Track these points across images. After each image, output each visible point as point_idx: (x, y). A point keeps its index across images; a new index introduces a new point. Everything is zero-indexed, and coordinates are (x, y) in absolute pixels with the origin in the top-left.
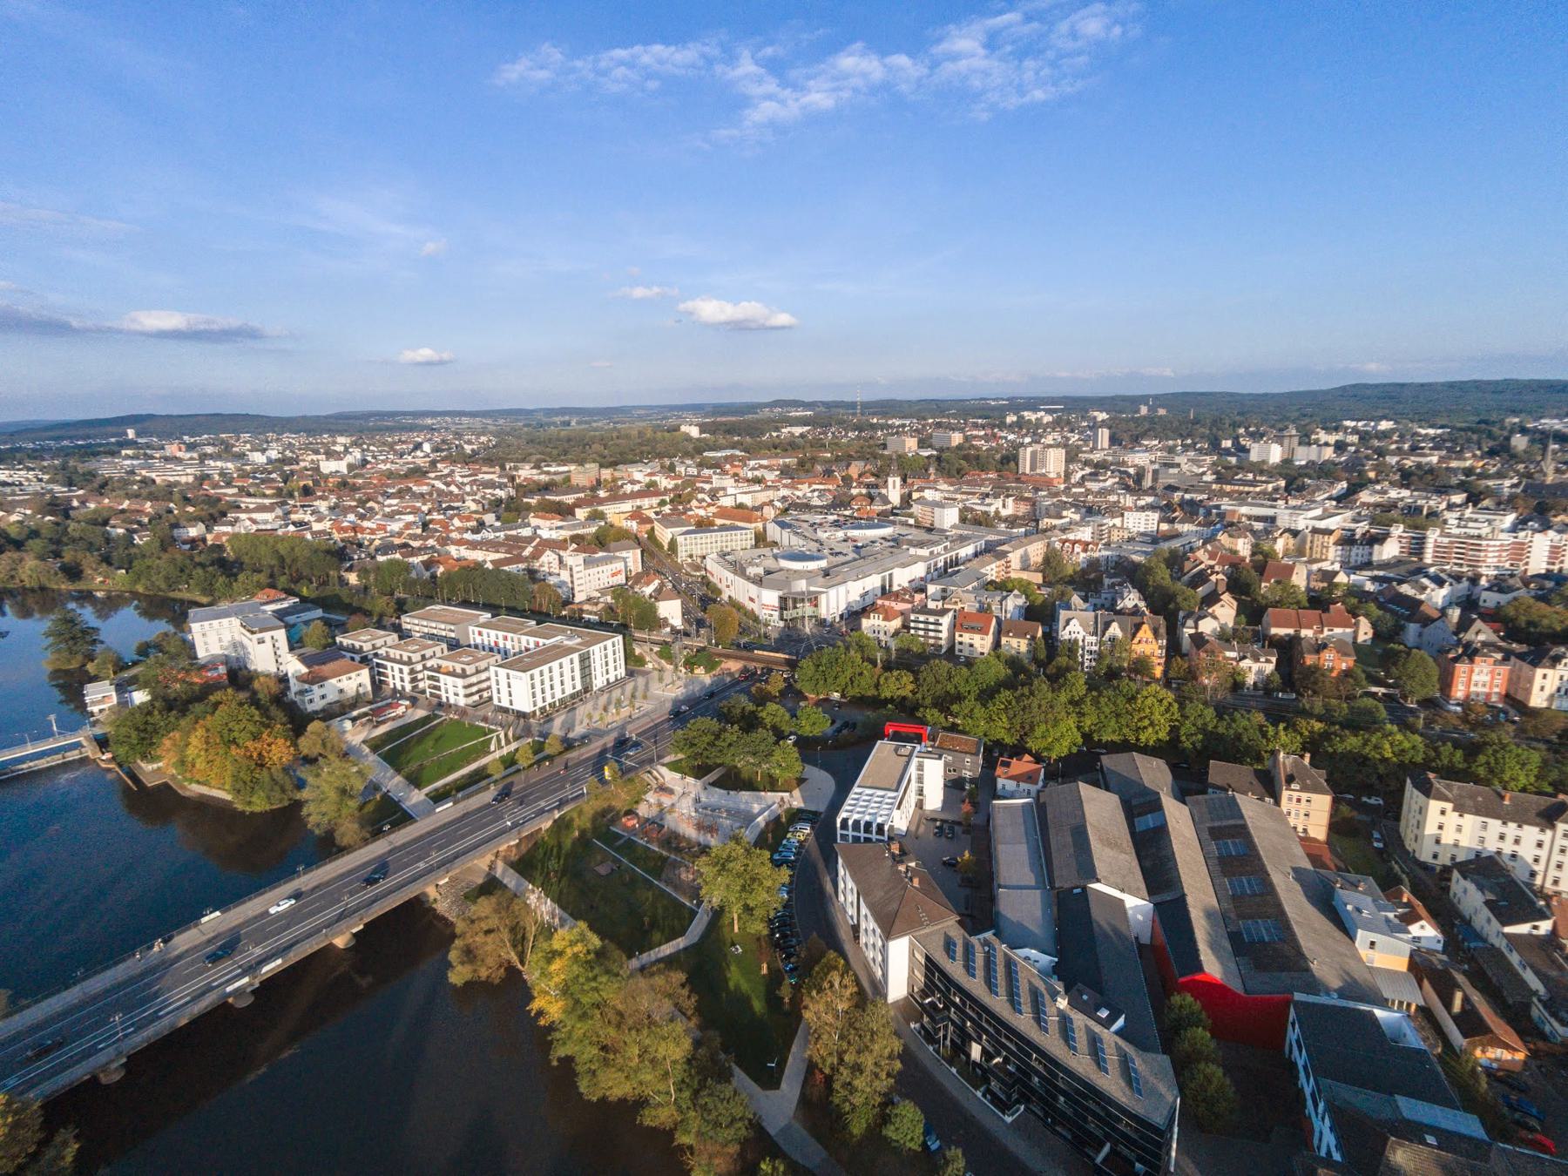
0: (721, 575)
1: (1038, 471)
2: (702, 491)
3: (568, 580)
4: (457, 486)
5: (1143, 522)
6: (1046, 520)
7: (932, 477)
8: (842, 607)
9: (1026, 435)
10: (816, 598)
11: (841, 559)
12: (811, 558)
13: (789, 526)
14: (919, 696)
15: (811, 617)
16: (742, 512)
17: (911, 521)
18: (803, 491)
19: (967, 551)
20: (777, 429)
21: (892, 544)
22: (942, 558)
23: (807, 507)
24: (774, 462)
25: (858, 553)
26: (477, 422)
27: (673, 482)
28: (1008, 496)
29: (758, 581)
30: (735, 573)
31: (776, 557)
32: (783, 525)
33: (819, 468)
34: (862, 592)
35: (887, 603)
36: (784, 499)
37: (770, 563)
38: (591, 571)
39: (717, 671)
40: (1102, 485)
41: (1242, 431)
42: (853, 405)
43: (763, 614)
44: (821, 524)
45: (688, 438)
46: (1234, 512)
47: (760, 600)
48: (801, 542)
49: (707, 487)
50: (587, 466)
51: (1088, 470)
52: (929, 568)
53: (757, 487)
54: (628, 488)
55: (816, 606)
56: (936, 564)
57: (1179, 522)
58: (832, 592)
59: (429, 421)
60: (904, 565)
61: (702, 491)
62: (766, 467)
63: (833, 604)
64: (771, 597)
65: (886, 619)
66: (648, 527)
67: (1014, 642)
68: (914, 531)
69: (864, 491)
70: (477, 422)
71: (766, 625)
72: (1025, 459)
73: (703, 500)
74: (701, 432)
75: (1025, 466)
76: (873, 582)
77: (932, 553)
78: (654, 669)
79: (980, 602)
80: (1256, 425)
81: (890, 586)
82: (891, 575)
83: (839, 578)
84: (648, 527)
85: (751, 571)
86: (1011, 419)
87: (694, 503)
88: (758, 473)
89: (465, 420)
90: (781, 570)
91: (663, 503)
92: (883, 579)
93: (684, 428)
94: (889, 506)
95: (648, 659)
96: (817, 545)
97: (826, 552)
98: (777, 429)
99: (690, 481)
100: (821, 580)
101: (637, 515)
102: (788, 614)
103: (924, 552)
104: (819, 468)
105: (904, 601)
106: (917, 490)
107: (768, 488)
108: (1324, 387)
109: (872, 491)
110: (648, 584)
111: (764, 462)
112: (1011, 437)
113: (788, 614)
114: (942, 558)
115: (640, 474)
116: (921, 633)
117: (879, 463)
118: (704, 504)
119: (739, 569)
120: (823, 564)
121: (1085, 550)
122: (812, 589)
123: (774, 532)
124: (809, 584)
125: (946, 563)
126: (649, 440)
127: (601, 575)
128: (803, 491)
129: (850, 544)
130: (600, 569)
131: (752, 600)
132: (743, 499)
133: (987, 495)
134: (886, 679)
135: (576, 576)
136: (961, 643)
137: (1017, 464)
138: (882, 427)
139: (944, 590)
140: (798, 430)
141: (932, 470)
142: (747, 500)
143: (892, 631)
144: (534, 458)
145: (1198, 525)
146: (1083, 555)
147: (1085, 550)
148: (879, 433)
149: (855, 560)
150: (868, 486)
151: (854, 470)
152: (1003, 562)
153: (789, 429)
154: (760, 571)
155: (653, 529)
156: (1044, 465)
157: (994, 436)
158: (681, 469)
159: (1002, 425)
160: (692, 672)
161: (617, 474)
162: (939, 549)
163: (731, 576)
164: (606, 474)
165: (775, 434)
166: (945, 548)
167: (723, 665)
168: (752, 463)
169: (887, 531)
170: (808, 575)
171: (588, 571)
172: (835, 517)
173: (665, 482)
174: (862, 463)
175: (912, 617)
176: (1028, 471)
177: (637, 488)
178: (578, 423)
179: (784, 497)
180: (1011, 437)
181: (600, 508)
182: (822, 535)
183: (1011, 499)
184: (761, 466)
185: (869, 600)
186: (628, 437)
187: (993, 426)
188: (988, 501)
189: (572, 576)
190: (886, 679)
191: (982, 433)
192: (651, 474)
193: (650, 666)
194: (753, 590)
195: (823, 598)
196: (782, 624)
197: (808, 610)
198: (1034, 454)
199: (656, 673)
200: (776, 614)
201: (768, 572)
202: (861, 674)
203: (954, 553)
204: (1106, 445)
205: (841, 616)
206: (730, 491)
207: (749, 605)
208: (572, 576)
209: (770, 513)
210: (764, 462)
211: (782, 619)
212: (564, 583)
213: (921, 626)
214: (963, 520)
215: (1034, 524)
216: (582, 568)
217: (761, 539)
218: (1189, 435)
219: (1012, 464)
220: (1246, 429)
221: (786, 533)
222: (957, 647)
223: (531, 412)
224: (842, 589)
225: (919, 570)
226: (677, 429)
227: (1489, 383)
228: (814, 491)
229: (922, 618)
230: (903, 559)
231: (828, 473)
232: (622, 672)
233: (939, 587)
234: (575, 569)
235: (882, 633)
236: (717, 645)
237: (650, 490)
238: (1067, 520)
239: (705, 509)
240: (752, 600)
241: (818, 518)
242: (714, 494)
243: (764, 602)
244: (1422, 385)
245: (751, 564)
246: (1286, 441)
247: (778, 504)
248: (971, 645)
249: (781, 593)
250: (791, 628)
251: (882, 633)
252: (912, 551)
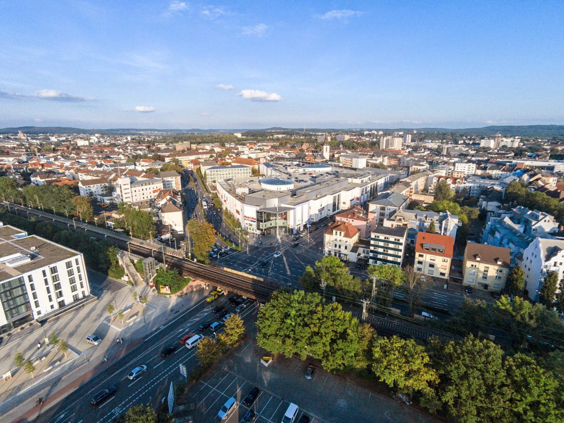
0: (223, 193)
1: (390, 148)
2: (233, 153)
3: (120, 194)
4: (123, 149)
5: (466, 169)
6: (414, 167)
7: (342, 149)
8: (306, 219)
9: (373, 138)
10: (286, 213)
11: (303, 184)
12: (283, 183)
13: (272, 166)
14: (449, 397)
15: (281, 227)
16: (249, 161)
17: (341, 165)
18: (281, 153)
19: (381, 182)
20: (272, 135)
21: (334, 176)
22: (369, 185)
23: (283, 159)
24: (269, 144)
25: (315, 181)
26: (160, 133)
27: (221, 150)
28: (384, 156)
29: (241, 199)
30: (229, 192)
31: (260, 182)
32: (267, 165)
33: (289, 146)
34: (320, 208)
35: (344, 219)
36: (271, 156)
37: (255, 186)
38: (137, 189)
39: (185, 290)
40: (422, 154)
41: (464, 138)
42: (302, 130)
43: (244, 224)
44: (289, 166)
45: (236, 137)
46: (523, 163)
47: (243, 213)
48: (278, 174)
49: (236, 151)
50: (185, 142)
51: (410, 150)
52: (362, 192)
53: (259, 151)
54: (201, 151)
55: (286, 219)
56: (366, 188)
57: (490, 169)
58: (298, 208)
59: (142, 132)
60: (348, 189)
61: (233, 153)
62: (267, 146)
63: (299, 217)
64: (251, 211)
65: (347, 235)
66: (198, 166)
67: (482, 267)
68: (343, 169)
69: (311, 154)
70: (160, 133)
71: (247, 233)
72: (383, 143)
73: (232, 156)
74: (242, 136)
75: (383, 146)
76: (328, 200)
77: (362, 181)
78: (129, 282)
79: (420, 220)
80: (470, 136)
81: (338, 204)
82: (339, 196)
83: (303, 198)
84: (198, 166)
85: (239, 191)
86: (366, 133)
87: (227, 157)
88: (261, 148)
89: (156, 132)
90: (262, 190)
91: (211, 156)
92: (335, 199)
93: (235, 134)
94: (324, 160)
95: (126, 271)
96: (288, 176)
97: (293, 179)
98: (272, 135)
99: (229, 151)
100: (289, 198)
101: (195, 162)
102: (263, 225)
103: (358, 181)
104: (289, 146)
105: (359, 218)
106: (337, 153)
107: (264, 151)
108: (481, 127)
109: (315, 154)
110: (162, 199)
111: (265, 144)
112: (367, 139)
113: (263, 225)
114: (369, 185)
115: (208, 147)
116: (381, 250)
117: (316, 144)
118: (232, 158)
119: (232, 191)
120: (291, 187)
121: (454, 182)
122: (283, 205)
123: (263, 169)
124: (280, 202)
125: (371, 188)
126: (220, 138)
127: (145, 191)
128: (281, 153)
129: (308, 176)
130: (144, 187)
131: (238, 212)
132: (250, 155)
133: (373, 156)
134: (385, 352)
135: (124, 192)
136: (420, 263)
137: (379, 145)
138: (314, 135)
139: (383, 209)
140: (280, 136)
141: (341, 146)
142: (253, 156)
143: (352, 245)
144: (168, 142)
145: (504, 170)
146: (452, 186)
147: (454, 182)
148: (313, 137)
149: (313, 185)
150: (312, 152)
151: (305, 146)
152: (408, 189)
153: (277, 135)
154: (246, 191)
155: (200, 167)
156: (392, 145)
157: (360, 139)
158: (227, 145)
159: (363, 135)
160: (158, 289)
161: (199, 147)
162: (365, 179)
163: (227, 194)
164: (194, 146)
165: (271, 137)
166: (369, 178)
167: (191, 283)
168: (259, 144)
169: (329, 169)
170: (280, 195)
171: (133, 189)
172: (297, 163)
173: (217, 150)
174: (308, 144)
175: (373, 235)
176: (384, 148)
177: (205, 151)
178: (198, 134)
179: (271, 155)
180: (367, 139)
181: (177, 158)
182: (290, 170)
183: (386, 157)
184: (263, 145)
185: (324, 215)
186: (212, 136)
187: (359, 136)
188: (374, 158)
189: (121, 192)
190: (385, 352)
191: (355, 137)
192: (212, 147)
193: (125, 278)
194: (239, 205)
195: (291, 213)
196: (259, 232)
197: (280, 222)
198: (387, 141)
199: (130, 286)
200: (255, 224)
201: (252, 192)
202: (343, 336)
203: (375, 182)
204: (410, 141)
205: (305, 226)
206: (246, 152)
207: (237, 216)
208: (121, 192)
209: (263, 161)
210: (265, 144)
211: (258, 229)
212: (119, 195)
213: (381, 244)
214: (367, 166)
215: (406, 169)
216: (129, 186)
217: (255, 173)
218: (443, 139)
219: (377, 145)
220: (466, 137)
221: (269, 170)
222: (416, 265)
223: (181, 130)
224: (305, 205)
225: (356, 193)
226: (233, 134)
227: (544, 126)
228: (287, 153)
229: (382, 237)
230: (345, 185)
231: (293, 147)
232: (87, 290)
233: (378, 206)
234: (123, 187)
235: (343, 248)
236: (193, 257)
237: (212, 151)
238: (425, 167)
239: (232, 160)
240: (238, 212)
241: (288, 163)
242: (238, 154)
243: (245, 215)
244: (519, 127)
245: (241, 186)
246: (496, 139)
247: (269, 158)
248: (432, 266)
249: (258, 208)
250: (266, 234)
251: (343, 248)
252: (350, 180)
